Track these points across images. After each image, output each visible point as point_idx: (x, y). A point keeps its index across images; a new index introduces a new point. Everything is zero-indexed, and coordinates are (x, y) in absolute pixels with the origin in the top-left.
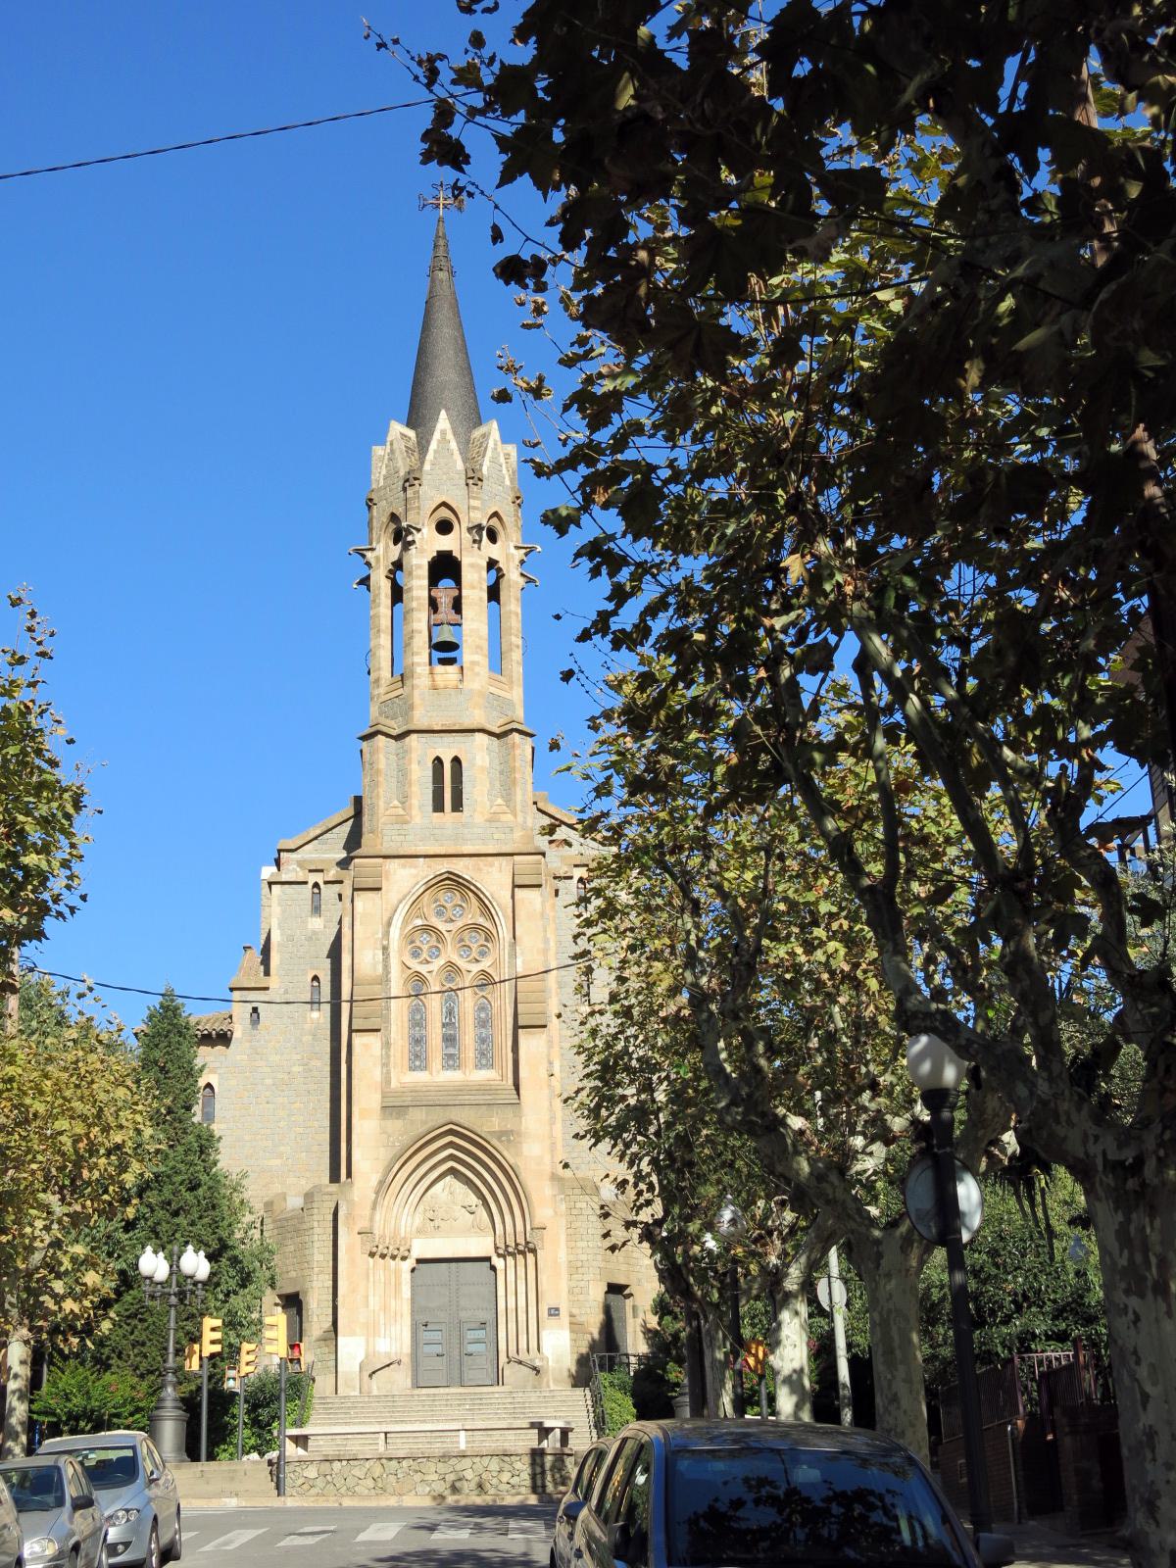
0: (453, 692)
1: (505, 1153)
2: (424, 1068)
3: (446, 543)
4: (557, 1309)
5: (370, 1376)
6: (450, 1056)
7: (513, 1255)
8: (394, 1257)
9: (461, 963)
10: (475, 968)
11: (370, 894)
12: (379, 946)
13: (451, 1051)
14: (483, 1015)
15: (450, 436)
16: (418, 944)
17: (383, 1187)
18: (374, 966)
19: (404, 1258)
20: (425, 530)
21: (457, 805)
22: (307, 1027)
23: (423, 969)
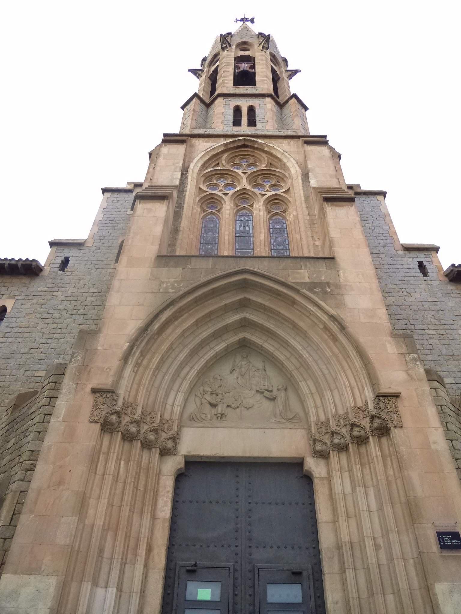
7: (342, 448)
8: (147, 445)
14: (278, 226)
19: (165, 453)
20: (234, 47)
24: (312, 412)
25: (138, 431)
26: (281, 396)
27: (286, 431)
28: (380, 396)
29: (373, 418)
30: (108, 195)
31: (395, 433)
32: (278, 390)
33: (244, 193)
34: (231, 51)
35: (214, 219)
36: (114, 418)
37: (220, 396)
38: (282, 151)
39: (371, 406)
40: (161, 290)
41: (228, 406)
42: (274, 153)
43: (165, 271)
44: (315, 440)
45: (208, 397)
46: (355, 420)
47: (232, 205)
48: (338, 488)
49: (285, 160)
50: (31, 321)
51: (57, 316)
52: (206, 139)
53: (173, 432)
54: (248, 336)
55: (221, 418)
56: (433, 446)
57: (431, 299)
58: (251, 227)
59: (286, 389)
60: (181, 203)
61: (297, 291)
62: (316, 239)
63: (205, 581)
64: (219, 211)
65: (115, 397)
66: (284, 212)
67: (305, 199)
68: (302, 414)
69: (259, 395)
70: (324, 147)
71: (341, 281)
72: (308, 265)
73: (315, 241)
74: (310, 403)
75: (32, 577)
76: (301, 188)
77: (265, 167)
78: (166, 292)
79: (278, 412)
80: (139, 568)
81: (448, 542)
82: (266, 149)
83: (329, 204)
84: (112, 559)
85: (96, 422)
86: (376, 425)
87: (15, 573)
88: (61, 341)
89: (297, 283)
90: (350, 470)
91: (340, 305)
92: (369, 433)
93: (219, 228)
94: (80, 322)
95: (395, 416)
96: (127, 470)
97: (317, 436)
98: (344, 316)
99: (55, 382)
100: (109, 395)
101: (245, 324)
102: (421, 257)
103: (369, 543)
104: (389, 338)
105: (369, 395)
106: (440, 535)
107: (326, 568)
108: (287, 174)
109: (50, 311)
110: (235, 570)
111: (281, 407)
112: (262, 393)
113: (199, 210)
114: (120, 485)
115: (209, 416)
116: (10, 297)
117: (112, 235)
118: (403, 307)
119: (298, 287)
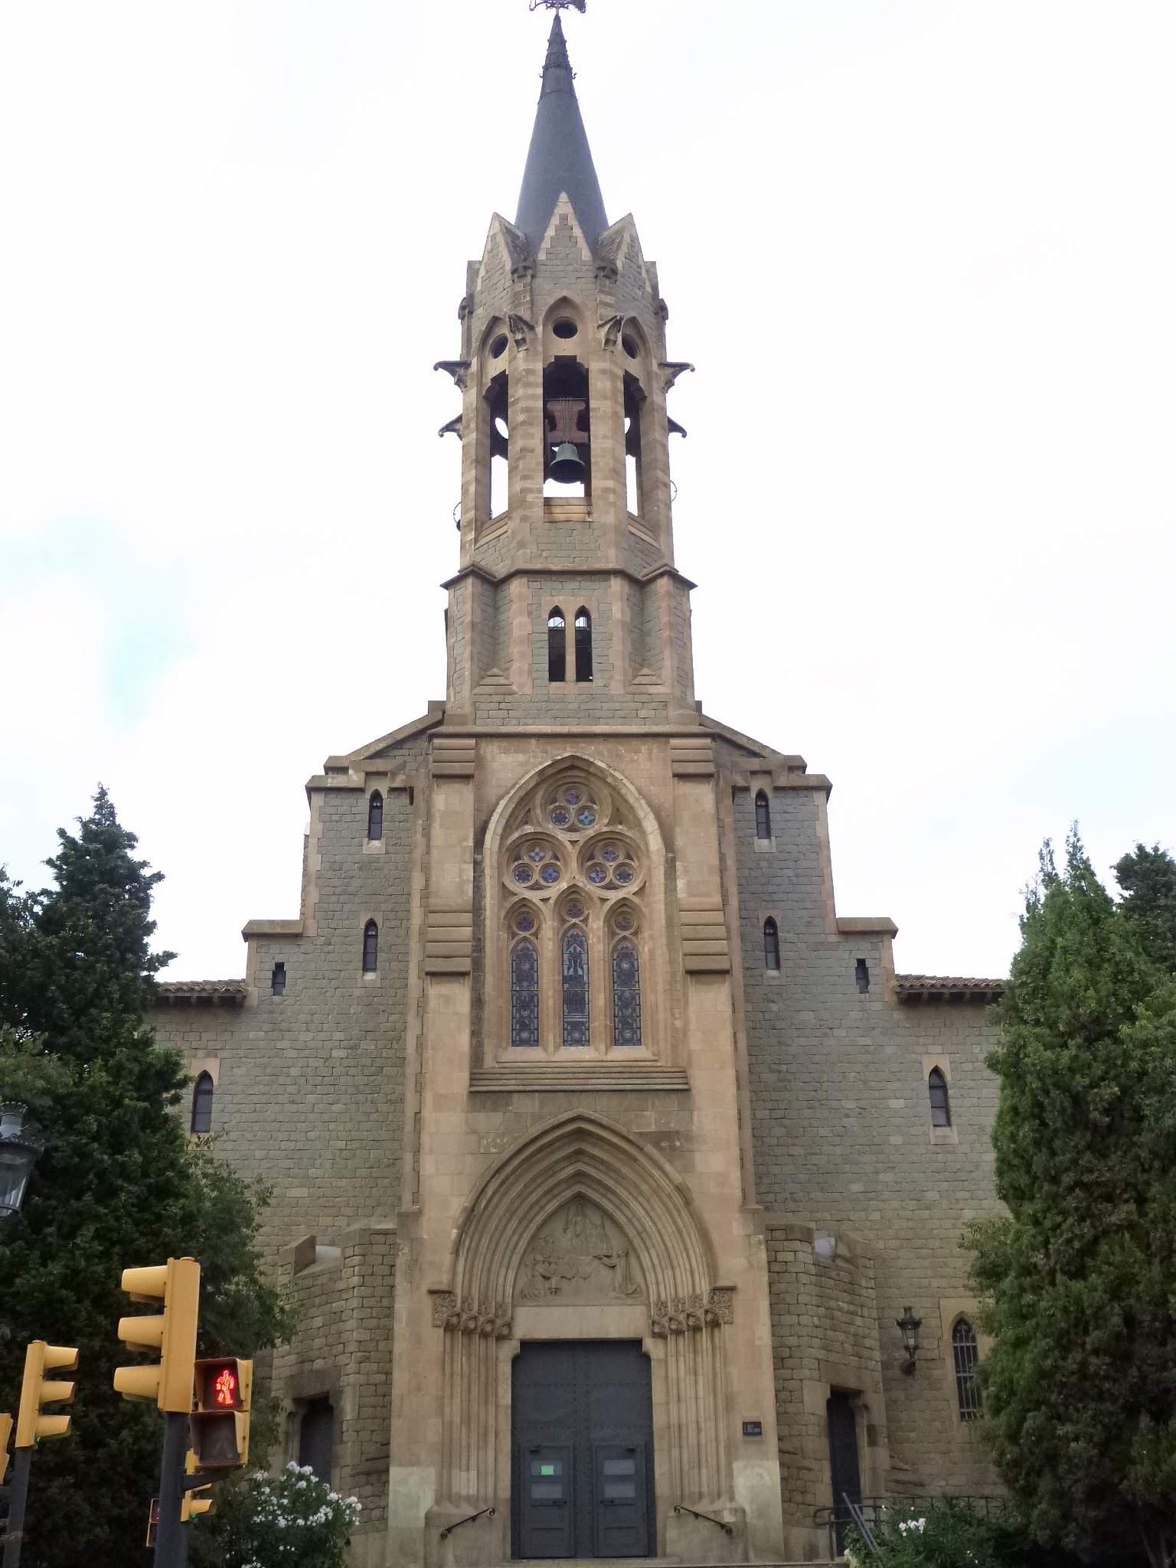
0: (579, 526)
1: (668, 1167)
2: (534, 1042)
3: (566, 347)
4: (758, 1425)
5: (443, 1536)
6: (576, 1026)
7: (678, 1333)
8: (485, 1335)
9: (593, 889)
10: (614, 896)
11: (457, 786)
12: (469, 856)
13: (577, 1018)
14: (625, 966)
15: (573, 221)
16: (526, 860)
17: (472, 1218)
18: (462, 883)
19: (500, 1338)
20: (539, 329)
21: (584, 672)
22: (357, 992)
23: (534, 896)
24: (653, 1288)
25: (476, 1328)
26: (621, 1264)
27: (626, 1309)
28: (715, 1290)
29: (707, 1312)
30: (318, 799)
31: (725, 1328)
32: (619, 1256)
33: (574, 892)
34: (536, 354)
35: (529, 950)
36: (454, 1320)
37: (553, 1265)
38: (636, 794)
39: (705, 1300)
40: (482, 1151)
41: (562, 1277)
42: (623, 791)
43: (481, 1116)
44: (653, 1323)
45: (540, 1268)
46: (691, 1310)
47: (556, 924)
48: (672, 1373)
49: (641, 814)
50: (255, 1099)
51: (292, 1089)
52: (504, 744)
53: (507, 1319)
54: (583, 1189)
55: (556, 1292)
56: (758, 1342)
57: (862, 1041)
58: (585, 967)
59: (627, 1255)
60: (480, 939)
61: (641, 1149)
62: (677, 1016)
63: (547, 1461)
64: (536, 935)
65: (453, 1298)
66: (635, 934)
67: (666, 923)
68: (643, 1286)
69: (596, 1261)
70: (707, 785)
71: (694, 1128)
72: (657, 1103)
73: (676, 1019)
74: (651, 1278)
75: (415, 1468)
76: (662, 896)
77: (608, 825)
78: (487, 1153)
79: (617, 1285)
80: (491, 1453)
81: (750, 1430)
82: (609, 780)
83: (694, 979)
84: (469, 1447)
85: (439, 1327)
86: (708, 1319)
87: (400, 1465)
88: (311, 1135)
89: (641, 1134)
90: (685, 1356)
91: (688, 1168)
92: (703, 1325)
93: (537, 971)
94: (331, 1098)
95: (727, 1311)
96: (470, 1365)
97: (656, 1318)
98: (692, 1183)
99: (364, 1255)
100: (447, 1295)
101: (580, 1176)
102: (864, 949)
103: (693, 1427)
104: (738, 1215)
105: (704, 1287)
106: (745, 1424)
107: (656, 1446)
108: (643, 847)
109: (281, 1080)
110: (575, 1448)
111: (620, 1279)
112: (601, 1259)
113: (506, 935)
114: (465, 1380)
115: (542, 1292)
116: (212, 1054)
117: (346, 907)
118: (817, 1058)
119: (641, 1143)
